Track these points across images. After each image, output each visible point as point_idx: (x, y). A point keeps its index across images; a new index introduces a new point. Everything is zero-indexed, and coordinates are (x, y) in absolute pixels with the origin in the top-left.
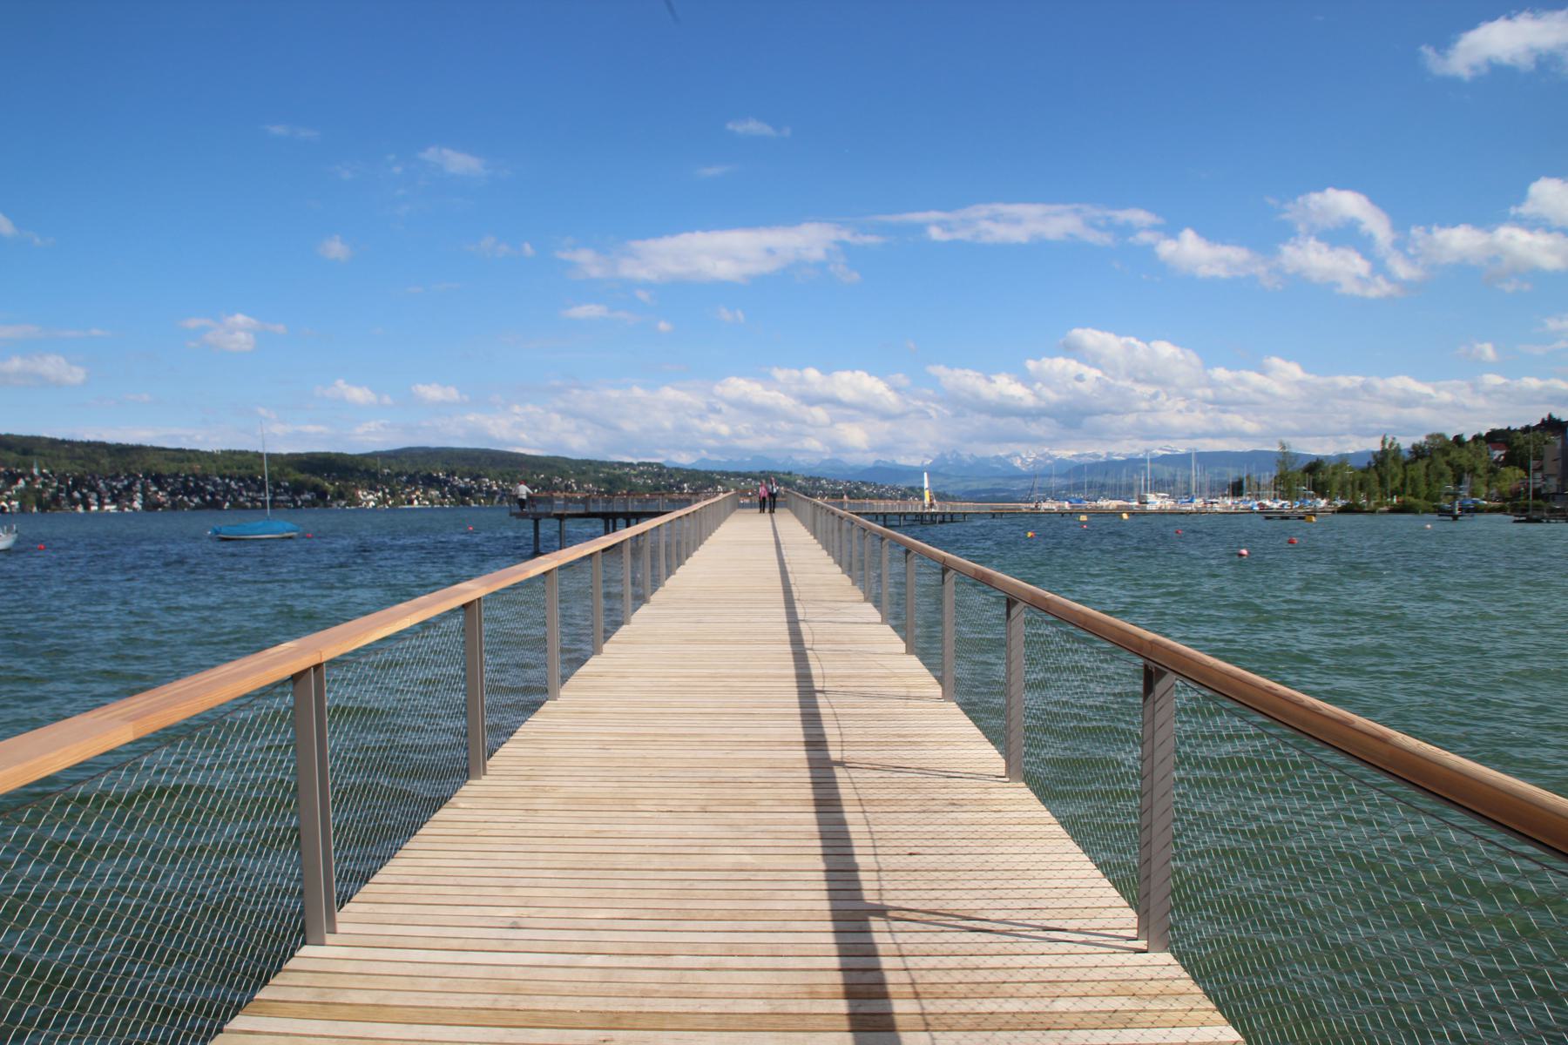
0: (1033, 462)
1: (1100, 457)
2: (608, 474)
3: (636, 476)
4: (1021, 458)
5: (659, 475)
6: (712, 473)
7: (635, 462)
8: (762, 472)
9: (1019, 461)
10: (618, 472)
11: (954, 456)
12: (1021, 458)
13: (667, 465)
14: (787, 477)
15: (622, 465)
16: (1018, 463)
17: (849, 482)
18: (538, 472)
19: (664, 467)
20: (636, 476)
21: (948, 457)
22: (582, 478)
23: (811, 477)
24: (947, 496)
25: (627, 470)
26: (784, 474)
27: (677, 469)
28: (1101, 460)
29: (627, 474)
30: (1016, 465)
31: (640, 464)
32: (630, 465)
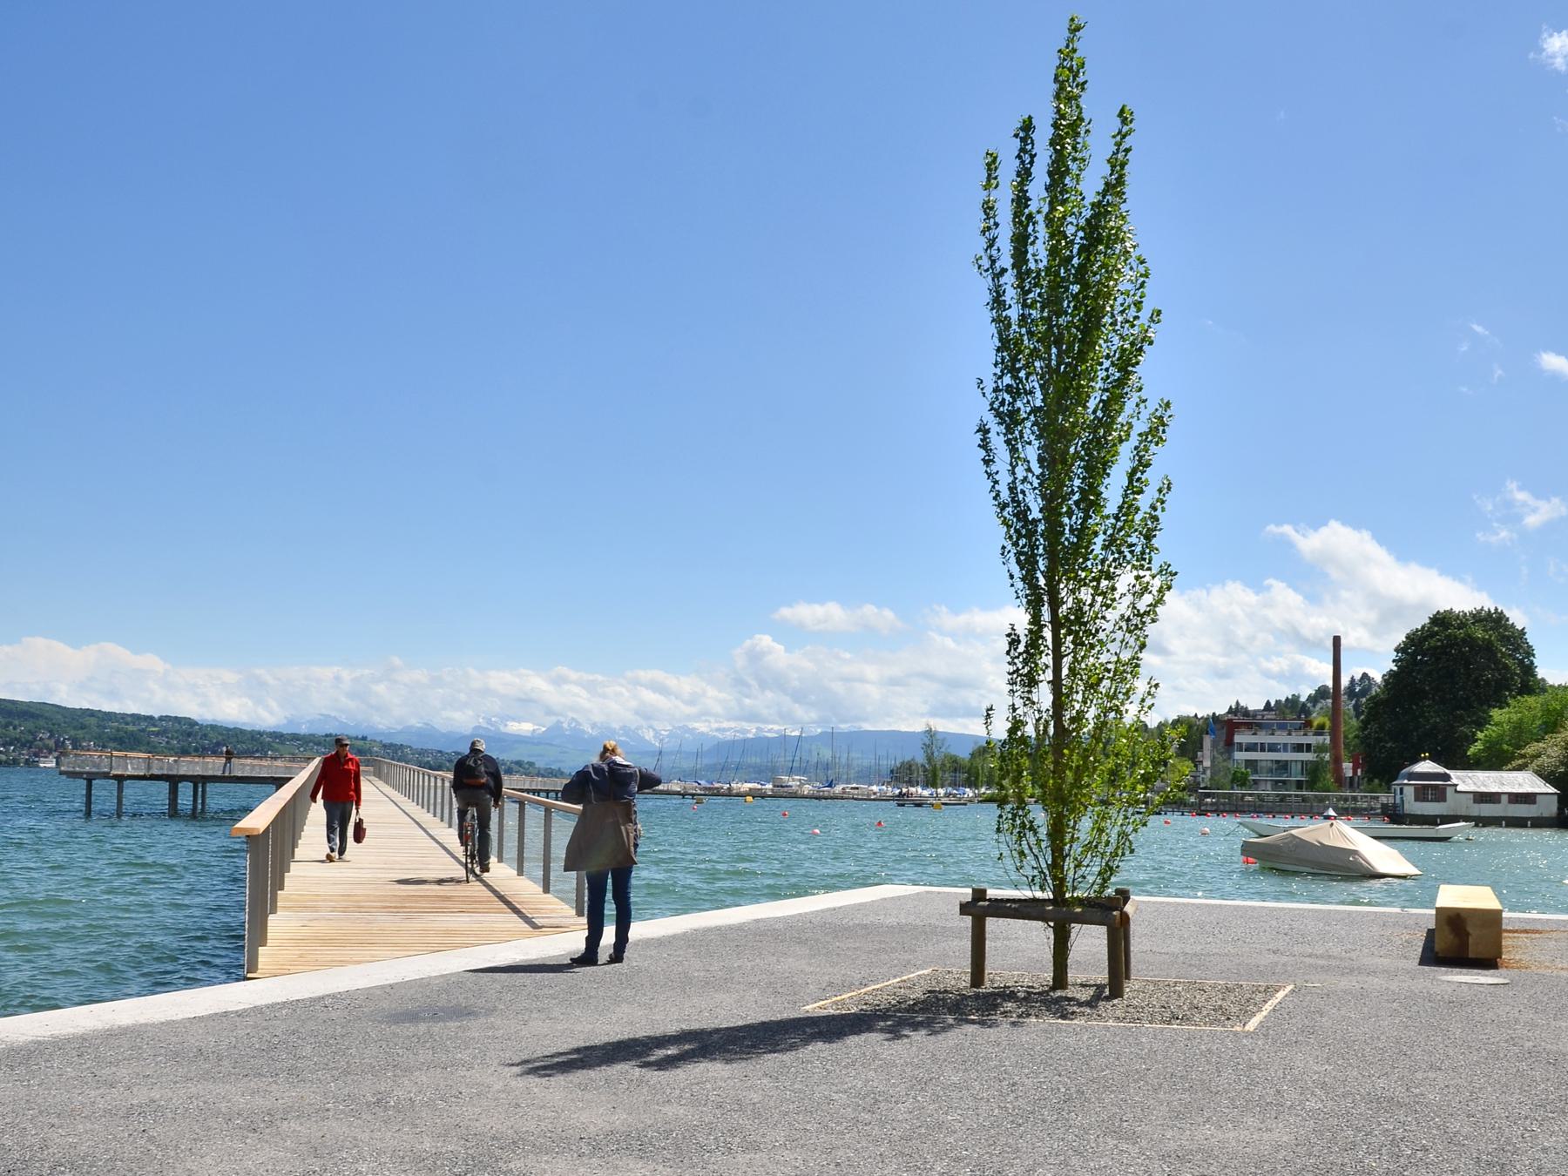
0: (668, 736)
1: (748, 731)
2: (118, 730)
3: (157, 734)
4: (654, 730)
5: (189, 735)
6: (261, 734)
7: (156, 716)
8: (327, 736)
9: (652, 733)
10: (131, 728)
11: (573, 725)
12: (654, 730)
13: (200, 723)
14: (362, 743)
15: (137, 718)
16: (649, 736)
17: (440, 752)
18: (17, 722)
19: (196, 724)
20: (157, 734)
21: (565, 725)
22: (80, 733)
23: (391, 745)
24: (562, 773)
25: (143, 725)
26: (357, 738)
27: (213, 727)
28: (750, 736)
29: (143, 731)
30: (647, 738)
31: (162, 718)
32: (151, 718)
